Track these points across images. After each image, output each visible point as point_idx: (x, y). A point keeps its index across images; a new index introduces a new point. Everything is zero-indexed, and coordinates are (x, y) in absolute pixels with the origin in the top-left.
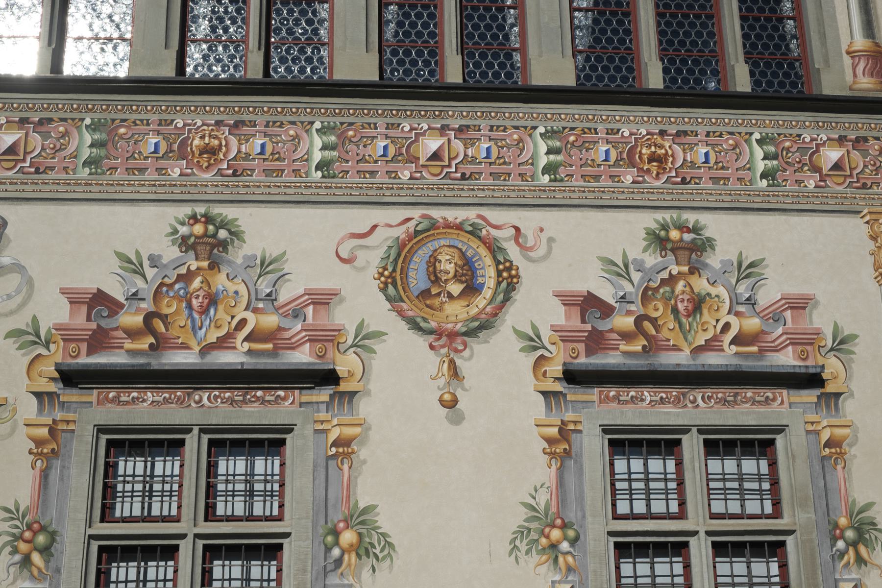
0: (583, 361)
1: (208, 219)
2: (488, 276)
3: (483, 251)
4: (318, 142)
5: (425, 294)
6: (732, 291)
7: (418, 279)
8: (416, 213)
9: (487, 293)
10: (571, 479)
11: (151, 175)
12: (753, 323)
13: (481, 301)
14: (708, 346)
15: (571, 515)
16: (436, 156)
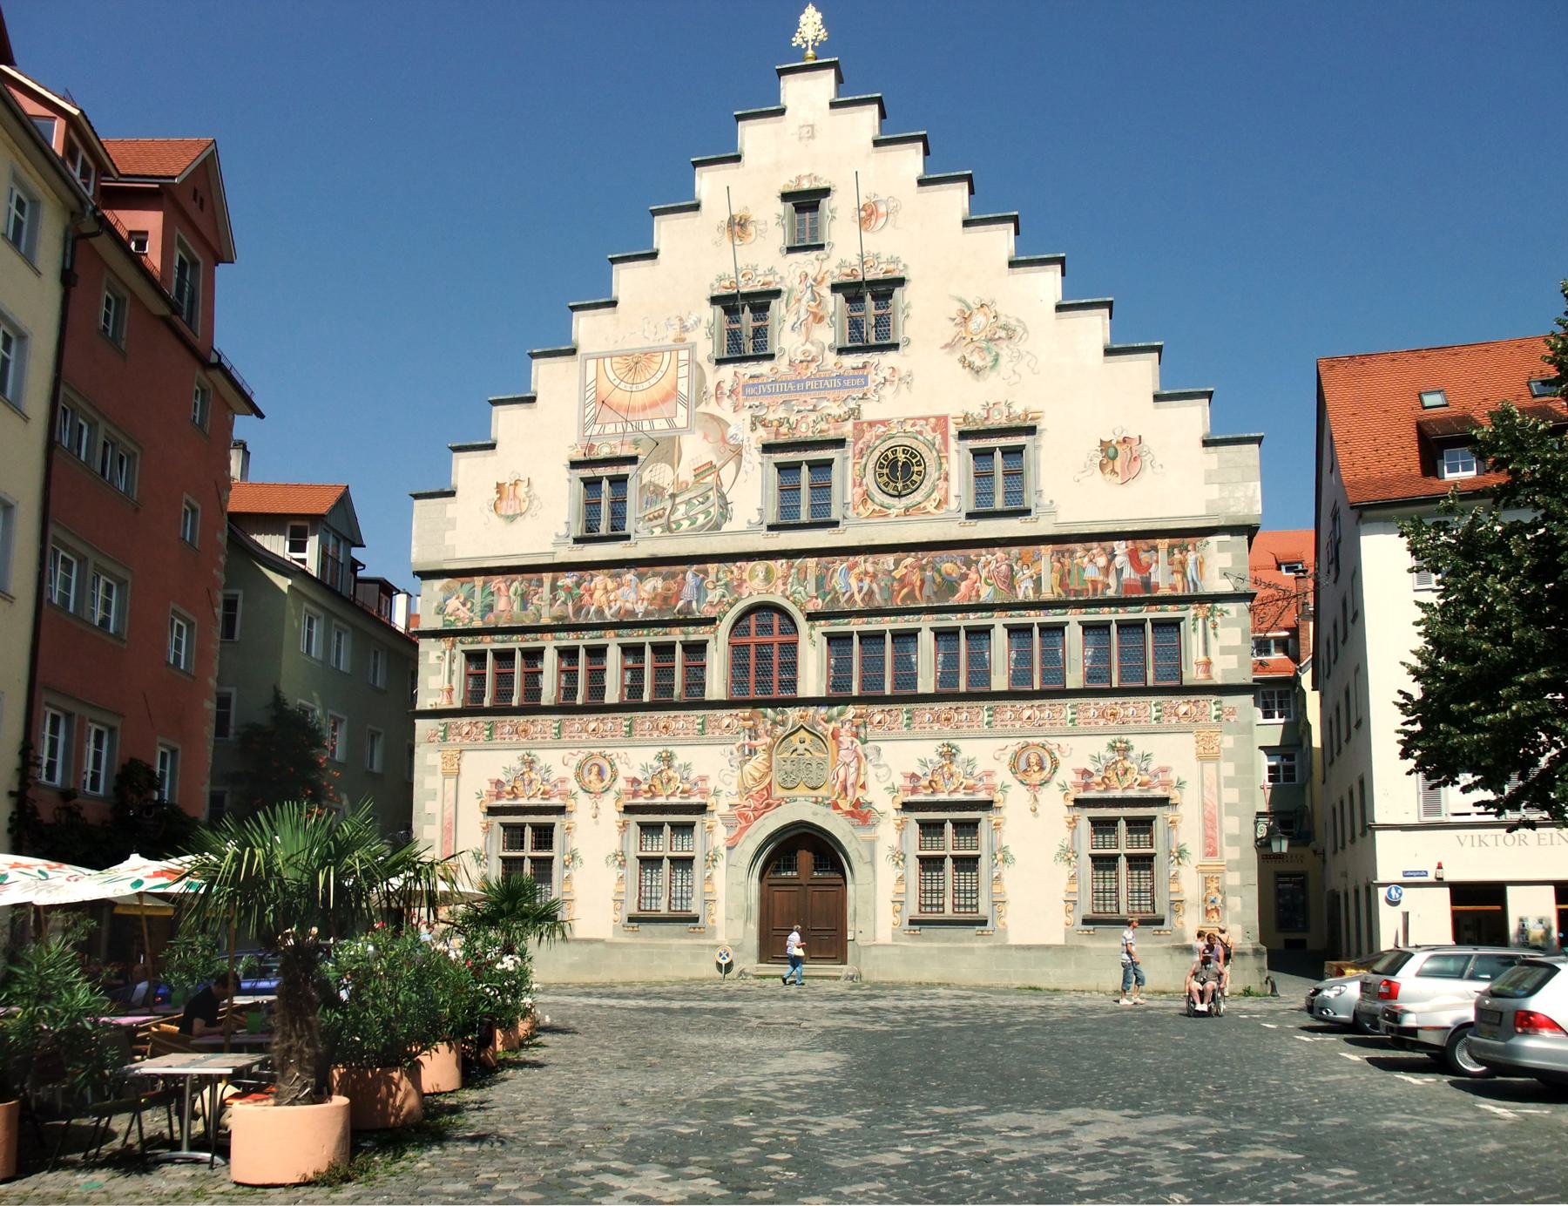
0: (1082, 795)
1: (949, 745)
2: (1048, 764)
3: (1047, 755)
4: (986, 714)
5: (1025, 771)
6: (1139, 766)
7: (1023, 766)
8: (1022, 740)
9: (1047, 770)
10: (1076, 837)
11: (928, 729)
12: (1146, 778)
13: (1045, 773)
14: (1128, 787)
15: (1076, 848)
16: (1029, 718)
